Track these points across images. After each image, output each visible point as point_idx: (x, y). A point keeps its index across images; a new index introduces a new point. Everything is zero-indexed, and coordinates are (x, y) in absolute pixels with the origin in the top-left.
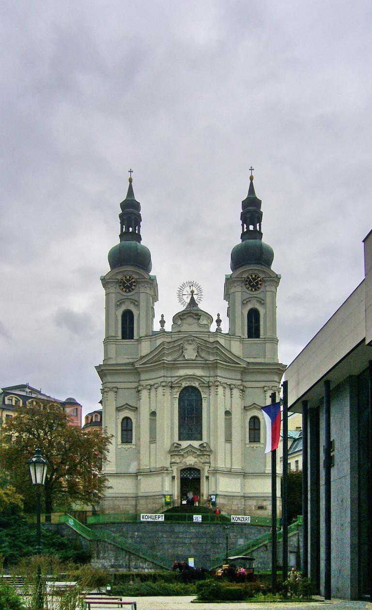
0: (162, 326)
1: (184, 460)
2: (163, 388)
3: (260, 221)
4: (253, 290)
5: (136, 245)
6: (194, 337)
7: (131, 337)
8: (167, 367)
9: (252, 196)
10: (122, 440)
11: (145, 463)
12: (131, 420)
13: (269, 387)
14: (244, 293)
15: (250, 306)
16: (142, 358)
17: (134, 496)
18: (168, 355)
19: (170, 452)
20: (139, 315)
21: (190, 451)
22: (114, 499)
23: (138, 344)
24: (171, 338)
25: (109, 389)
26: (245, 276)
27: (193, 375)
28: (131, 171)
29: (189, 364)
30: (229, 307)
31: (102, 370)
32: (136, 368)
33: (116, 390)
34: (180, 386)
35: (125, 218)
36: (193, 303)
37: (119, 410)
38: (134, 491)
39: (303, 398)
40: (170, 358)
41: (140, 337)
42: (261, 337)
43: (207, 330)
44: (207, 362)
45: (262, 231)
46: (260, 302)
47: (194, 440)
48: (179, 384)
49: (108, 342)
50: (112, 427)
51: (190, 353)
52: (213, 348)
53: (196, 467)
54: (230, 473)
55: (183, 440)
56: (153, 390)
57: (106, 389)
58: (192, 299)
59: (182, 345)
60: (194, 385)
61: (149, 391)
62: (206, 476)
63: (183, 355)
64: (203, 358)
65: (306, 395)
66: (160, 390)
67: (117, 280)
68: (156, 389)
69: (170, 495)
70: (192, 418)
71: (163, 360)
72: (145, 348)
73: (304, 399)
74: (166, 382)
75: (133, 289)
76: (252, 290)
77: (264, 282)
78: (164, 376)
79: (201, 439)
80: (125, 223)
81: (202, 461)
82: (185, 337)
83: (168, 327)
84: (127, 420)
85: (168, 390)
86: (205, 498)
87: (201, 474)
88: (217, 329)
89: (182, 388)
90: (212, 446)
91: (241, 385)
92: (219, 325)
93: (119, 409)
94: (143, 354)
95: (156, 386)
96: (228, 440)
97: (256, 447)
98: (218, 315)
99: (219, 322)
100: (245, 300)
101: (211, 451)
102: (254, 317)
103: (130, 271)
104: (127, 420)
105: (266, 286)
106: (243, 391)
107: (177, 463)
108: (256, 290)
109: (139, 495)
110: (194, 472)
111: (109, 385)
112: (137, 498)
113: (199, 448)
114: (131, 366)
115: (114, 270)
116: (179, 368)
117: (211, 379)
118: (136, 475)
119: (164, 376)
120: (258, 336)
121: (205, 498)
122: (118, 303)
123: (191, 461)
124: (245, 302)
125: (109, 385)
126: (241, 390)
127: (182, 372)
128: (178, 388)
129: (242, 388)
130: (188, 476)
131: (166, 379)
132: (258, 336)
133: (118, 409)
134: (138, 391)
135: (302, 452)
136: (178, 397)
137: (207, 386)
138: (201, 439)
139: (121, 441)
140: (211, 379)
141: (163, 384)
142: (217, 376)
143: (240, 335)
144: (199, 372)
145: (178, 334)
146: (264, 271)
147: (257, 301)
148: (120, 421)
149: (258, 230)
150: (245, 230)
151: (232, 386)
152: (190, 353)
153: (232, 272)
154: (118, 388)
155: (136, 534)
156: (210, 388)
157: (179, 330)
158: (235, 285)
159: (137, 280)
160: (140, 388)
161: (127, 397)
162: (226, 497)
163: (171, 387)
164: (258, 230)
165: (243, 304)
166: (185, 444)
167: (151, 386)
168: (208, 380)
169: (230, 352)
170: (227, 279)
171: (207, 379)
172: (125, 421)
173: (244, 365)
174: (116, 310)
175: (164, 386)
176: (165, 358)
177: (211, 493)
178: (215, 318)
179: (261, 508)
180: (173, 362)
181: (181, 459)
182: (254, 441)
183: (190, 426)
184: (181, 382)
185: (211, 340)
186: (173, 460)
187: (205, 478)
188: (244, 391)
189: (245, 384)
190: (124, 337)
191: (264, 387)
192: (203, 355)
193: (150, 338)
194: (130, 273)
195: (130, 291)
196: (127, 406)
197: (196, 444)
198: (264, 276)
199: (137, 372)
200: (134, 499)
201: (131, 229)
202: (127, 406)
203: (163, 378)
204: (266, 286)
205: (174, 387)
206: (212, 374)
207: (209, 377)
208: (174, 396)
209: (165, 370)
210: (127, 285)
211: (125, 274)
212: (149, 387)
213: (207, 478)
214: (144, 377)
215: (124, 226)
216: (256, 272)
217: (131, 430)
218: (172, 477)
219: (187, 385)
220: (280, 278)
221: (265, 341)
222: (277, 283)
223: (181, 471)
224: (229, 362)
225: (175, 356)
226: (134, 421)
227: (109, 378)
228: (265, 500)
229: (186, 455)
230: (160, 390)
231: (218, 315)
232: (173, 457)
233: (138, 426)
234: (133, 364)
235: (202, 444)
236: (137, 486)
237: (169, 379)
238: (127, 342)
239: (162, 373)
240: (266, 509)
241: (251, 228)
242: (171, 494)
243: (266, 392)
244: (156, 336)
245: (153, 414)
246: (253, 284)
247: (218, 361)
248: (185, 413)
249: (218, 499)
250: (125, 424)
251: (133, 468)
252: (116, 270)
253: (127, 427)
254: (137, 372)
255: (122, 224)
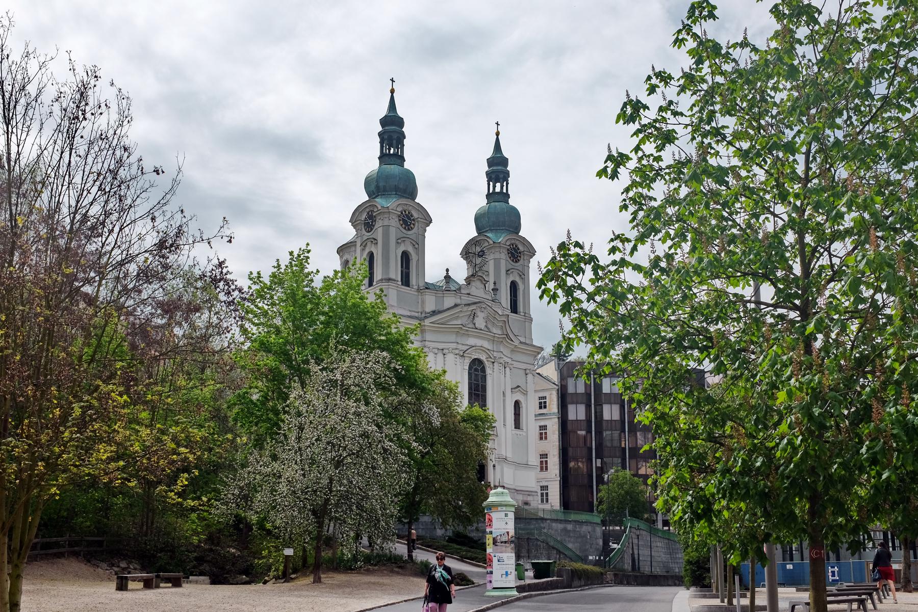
28: (392, 80)
35: (386, 137)
51: (480, 322)
66: (450, 357)
85: (459, 359)
95: (445, 351)
117: (495, 354)
127: (472, 341)
141: (457, 352)
144: (486, 344)
173: (516, 343)
192: (489, 326)
195: (409, 230)
212: (436, 351)
213: (494, 466)
239: (453, 338)
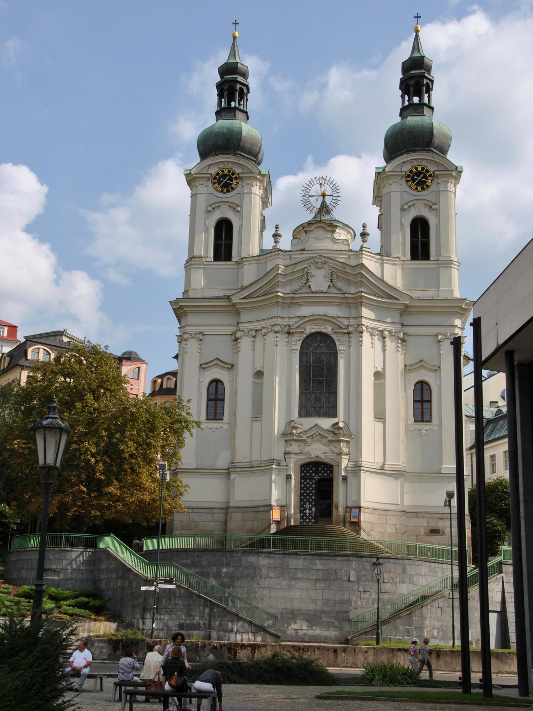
0: (276, 242)
1: (307, 449)
2: (276, 335)
3: (429, 90)
4: (419, 188)
5: (238, 126)
6: (327, 257)
7: (228, 258)
8: (283, 303)
9: (415, 55)
10: (207, 416)
11: (244, 453)
12: (223, 384)
13: (444, 335)
14: (406, 193)
15: (413, 214)
16: (243, 289)
17: (224, 506)
18: (285, 284)
19: (284, 434)
20: (242, 225)
21: (317, 434)
22: (190, 511)
23: (238, 268)
24: (290, 259)
25: (189, 336)
26: (407, 168)
27: (325, 315)
28: (236, 23)
29: (317, 298)
30: (381, 215)
31: (181, 307)
32: (234, 305)
33: (201, 338)
34: (302, 333)
36: (324, 209)
37: (204, 368)
38: (224, 499)
39: (507, 345)
40: (287, 289)
41: (242, 259)
42: (431, 258)
43: (346, 248)
44: (346, 295)
45: (433, 104)
46: (431, 207)
47: (324, 416)
48: (302, 328)
49: (191, 265)
50: (193, 397)
51: (319, 281)
52: (355, 275)
53: (326, 461)
54: (381, 471)
55: (306, 416)
56: (259, 339)
57: (186, 336)
58: (323, 204)
59: (306, 270)
60: (324, 331)
61: (253, 339)
62: (343, 476)
63: (308, 285)
64: (339, 289)
65: (510, 343)
66: (271, 337)
67: (209, 176)
68: (264, 335)
69: (282, 506)
70: (321, 382)
71: (277, 292)
72: (249, 274)
73: (507, 347)
74: (280, 325)
75: (233, 189)
76: (417, 189)
77: (436, 177)
78: (277, 317)
79: (335, 415)
80: (226, 93)
81: (336, 451)
82: (311, 258)
83: (285, 243)
84: (216, 384)
86: (341, 511)
87: (335, 472)
88: (362, 247)
89: (305, 336)
90: (352, 430)
91: (399, 332)
92: (364, 241)
93: (203, 367)
94: (246, 284)
95: (264, 331)
96: (380, 415)
97: (426, 431)
98: (364, 226)
99: (364, 235)
100: (406, 204)
101: (350, 435)
102: (420, 230)
103: (229, 162)
104: (216, 384)
105: (439, 183)
106: (403, 340)
107: (296, 454)
108: (423, 189)
109: (231, 505)
110: (323, 469)
111: (188, 329)
112: (227, 509)
113: (331, 429)
114: (226, 300)
115: (205, 161)
116: (299, 304)
117: (353, 322)
118: (228, 472)
119: (277, 317)
120: (426, 256)
121: (341, 511)
122: (210, 208)
123: (318, 451)
124: (406, 207)
125: (188, 329)
126: (400, 339)
127: (306, 311)
128: (299, 335)
129: (401, 336)
130: (314, 475)
131: (280, 321)
132: (426, 256)
133: (203, 366)
134: (236, 340)
135: (506, 440)
136: (299, 349)
137: (345, 333)
138: (335, 415)
139: (205, 418)
140: (353, 322)
141: (277, 328)
142: (362, 317)
143: (400, 256)
144: (332, 311)
145: (302, 254)
146: (436, 162)
147: (425, 204)
148: (206, 384)
149: (427, 103)
150: (407, 103)
151: (386, 333)
152: (319, 281)
153: (385, 164)
154: (204, 335)
155: (224, 570)
156: (351, 335)
157: (302, 248)
158: (391, 182)
159: (240, 175)
160: (239, 334)
161: (219, 348)
162: (376, 512)
163: (289, 333)
164: (427, 103)
165: (403, 209)
166: (309, 422)
167: (257, 331)
168: (348, 324)
169: (382, 280)
170: (378, 174)
171: (345, 322)
172: (214, 385)
174: (206, 218)
175: (277, 332)
176: (280, 290)
177: (350, 504)
178: (359, 230)
179: (435, 531)
180: (292, 295)
181: (301, 447)
182: (422, 421)
183: (318, 396)
184: (303, 326)
185: (353, 263)
186: (289, 449)
187: (341, 479)
188: (405, 341)
189: (406, 329)
190: (217, 257)
191: (437, 335)
192: (339, 285)
193: (258, 260)
194: (229, 166)
195: (228, 191)
196: (218, 362)
197: (326, 423)
198: (436, 169)
199: (235, 310)
200: (224, 511)
201: (233, 104)
202: (218, 362)
203: (276, 320)
204: (439, 183)
205: (293, 333)
206: (354, 314)
207: (348, 318)
208: (294, 347)
209: (279, 308)
210: (225, 182)
211: (222, 166)
212: (253, 333)
214: (244, 317)
215: (223, 100)
216: (424, 163)
217: (223, 400)
218: (287, 475)
219: (313, 331)
220: (461, 172)
221: (438, 264)
222: (457, 179)
223: (302, 466)
224: (381, 297)
225: (296, 286)
226: (227, 385)
227: (191, 319)
228: (441, 519)
229: (309, 440)
230: (271, 337)
231: (364, 226)
232: (289, 443)
233: (235, 394)
234: (229, 298)
235: (337, 423)
236: (228, 492)
237: (286, 321)
238: (222, 265)
240: (444, 534)
241: (416, 100)
242: (284, 504)
243: (441, 343)
244: (267, 256)
245: (259, 374)
246: (419, 179)
247: (363, 294)
248: (310, 375)
249: (362, 514)
250: (213, 390)
251: (223, 462)
252: (210, 161)
253: (216, 395)
254: (235, 310)
255: (220, 96)
